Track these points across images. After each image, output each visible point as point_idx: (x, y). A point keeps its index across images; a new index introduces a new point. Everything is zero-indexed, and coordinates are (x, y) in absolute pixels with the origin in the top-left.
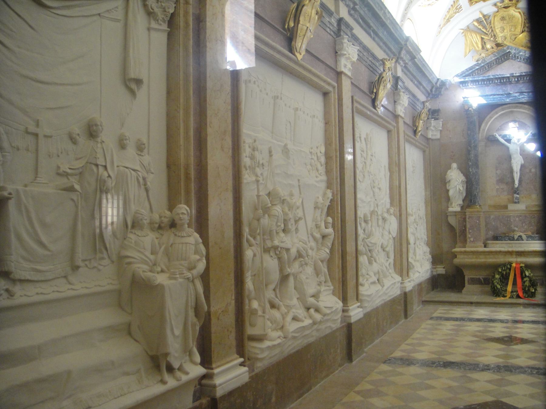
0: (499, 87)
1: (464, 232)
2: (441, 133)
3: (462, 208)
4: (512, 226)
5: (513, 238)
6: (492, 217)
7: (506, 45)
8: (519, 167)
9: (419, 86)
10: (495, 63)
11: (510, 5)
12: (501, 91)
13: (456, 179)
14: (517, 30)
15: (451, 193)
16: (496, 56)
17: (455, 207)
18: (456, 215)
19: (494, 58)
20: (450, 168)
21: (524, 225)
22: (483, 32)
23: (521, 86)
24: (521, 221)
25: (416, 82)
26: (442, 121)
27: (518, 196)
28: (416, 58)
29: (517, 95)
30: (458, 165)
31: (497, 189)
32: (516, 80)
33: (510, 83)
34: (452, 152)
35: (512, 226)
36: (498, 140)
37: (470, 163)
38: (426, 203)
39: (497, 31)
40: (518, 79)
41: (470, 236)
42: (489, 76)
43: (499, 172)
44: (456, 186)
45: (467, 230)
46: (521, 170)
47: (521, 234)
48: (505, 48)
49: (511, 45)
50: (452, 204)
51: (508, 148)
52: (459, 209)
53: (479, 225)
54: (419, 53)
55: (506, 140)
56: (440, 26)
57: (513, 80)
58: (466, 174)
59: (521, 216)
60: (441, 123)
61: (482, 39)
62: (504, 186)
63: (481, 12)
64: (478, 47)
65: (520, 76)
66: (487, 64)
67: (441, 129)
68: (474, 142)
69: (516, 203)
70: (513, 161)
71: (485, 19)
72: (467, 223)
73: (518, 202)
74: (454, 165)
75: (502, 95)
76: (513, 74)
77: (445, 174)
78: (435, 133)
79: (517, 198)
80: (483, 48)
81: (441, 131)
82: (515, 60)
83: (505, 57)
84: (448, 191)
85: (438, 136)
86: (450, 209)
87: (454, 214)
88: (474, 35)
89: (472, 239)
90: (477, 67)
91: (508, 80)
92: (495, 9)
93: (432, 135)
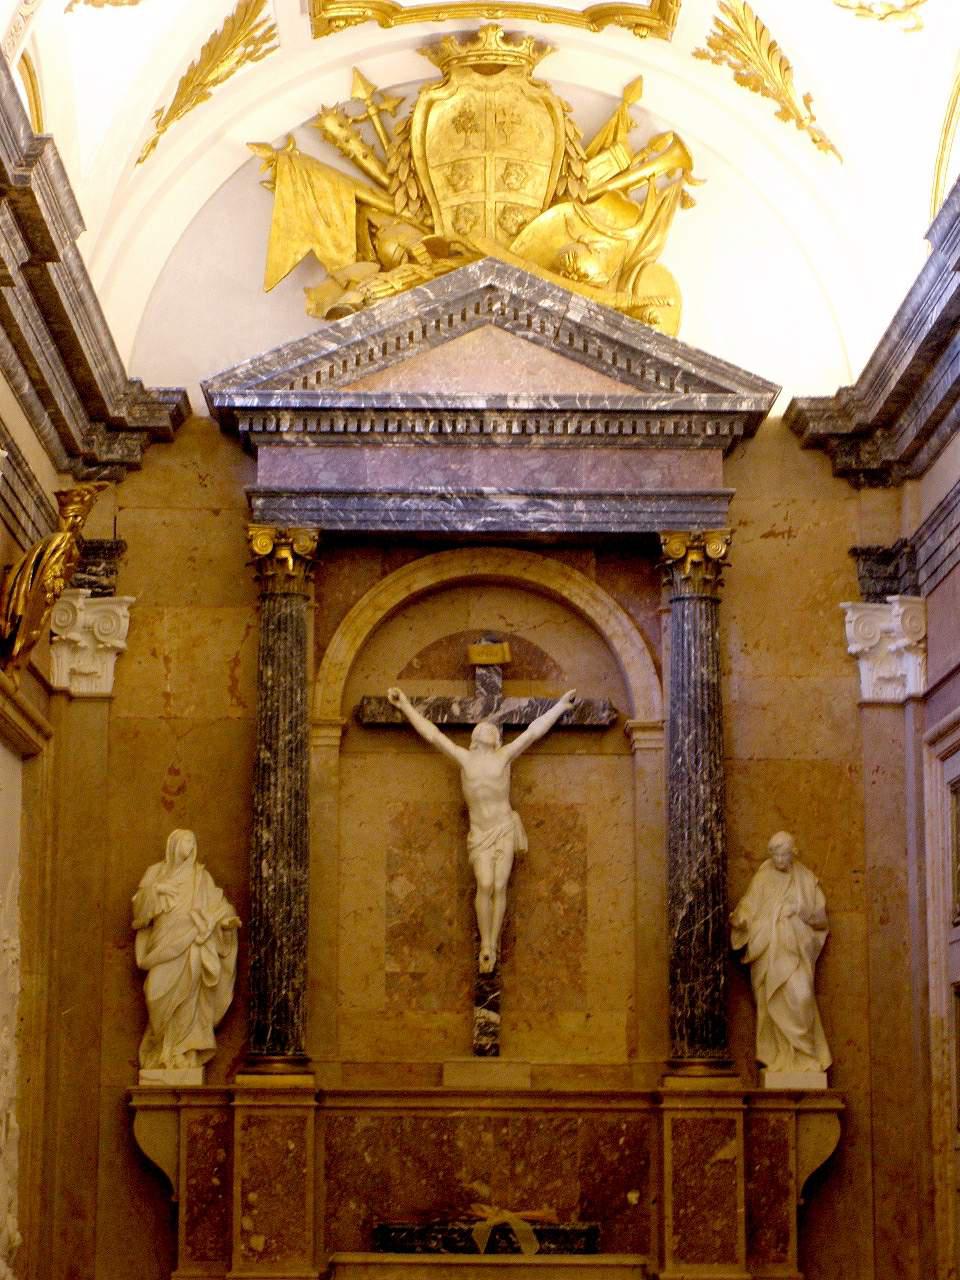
0: (431, 458)
1: (214, 1205)
2: (117, 668)
3: (208, 1067)
4: (462, 1174)
5: (467, 1235)
6: (362, 1122)
7: (481, 255)
8: (504, 868)
9: (37, 407)
10: (418, 334)
11: (509, 61)
12: (437, 476)
13: (188, 912)
14: (529, 188)
15: (157, 986)
16: (428, 301)
17: (176, 1063)
18: (176, 1109)
19: (413, 311)
20: (159, 853)
21: (519, 1169)
22: (367, 173)
23: (535, 464)
24: (505, 1145)
25: (26, 387)
26: (131, 608)
27: (494, 1017)
28: (54, 258)
29: (512, 503)
30: (200, 843)
31: (390, 976)
32: (516, 429)
33: (486, 440)
34: (174, 772)
35: (462, 1174)
36: (406, 728)
37: (266, 836)
38: (23, 1036)
39: (437, 178)
40: (524, 428)
41: (248, 1224)
42: (388, 396)
43: (402, 887)
44: (184, 953)
45: (237, 1189)
46: (511, 883)
47: (507, 1216)
48: (472, 268)
49: (501, 255)
50: (156, 1046)
51: (455, 772)
52: (192, 1076)
53: (300, 1163)
54: (74, 236)
55: (442, 728)
56: (159, 112)
57: (503, 429)
58: (244, 896)
59: (505, 1122)
60: (123, 611)
61: (359, 202)
62: (423, 961)
63: (359, 75)
64: (339, 247)
65: (539, 411)
66: (381, 334)
67: (121, 644)
68: (293, 727)
69: (480, 1051)
70: (477, 836)
71: (380, 112)
72: (238, 1151)
73: (496, 1051)
74: (184, 841)
75: (442, 497)
76: (504, 398)
77: (135, 888)
78: (84, 663)
79: (486, 1029)
80: (361, 255)
81: (120, 653)
82: (512, 331)
83: (470, 314)
84: (140, 975)
85: (104, 685)
86: (150, 1076)
87: (169, 1101)
88: (323, 184)
89: (258, 1242)
90: (333, 347)
91: (475, 428)
92: (428, 69)
93: (73, 673)
